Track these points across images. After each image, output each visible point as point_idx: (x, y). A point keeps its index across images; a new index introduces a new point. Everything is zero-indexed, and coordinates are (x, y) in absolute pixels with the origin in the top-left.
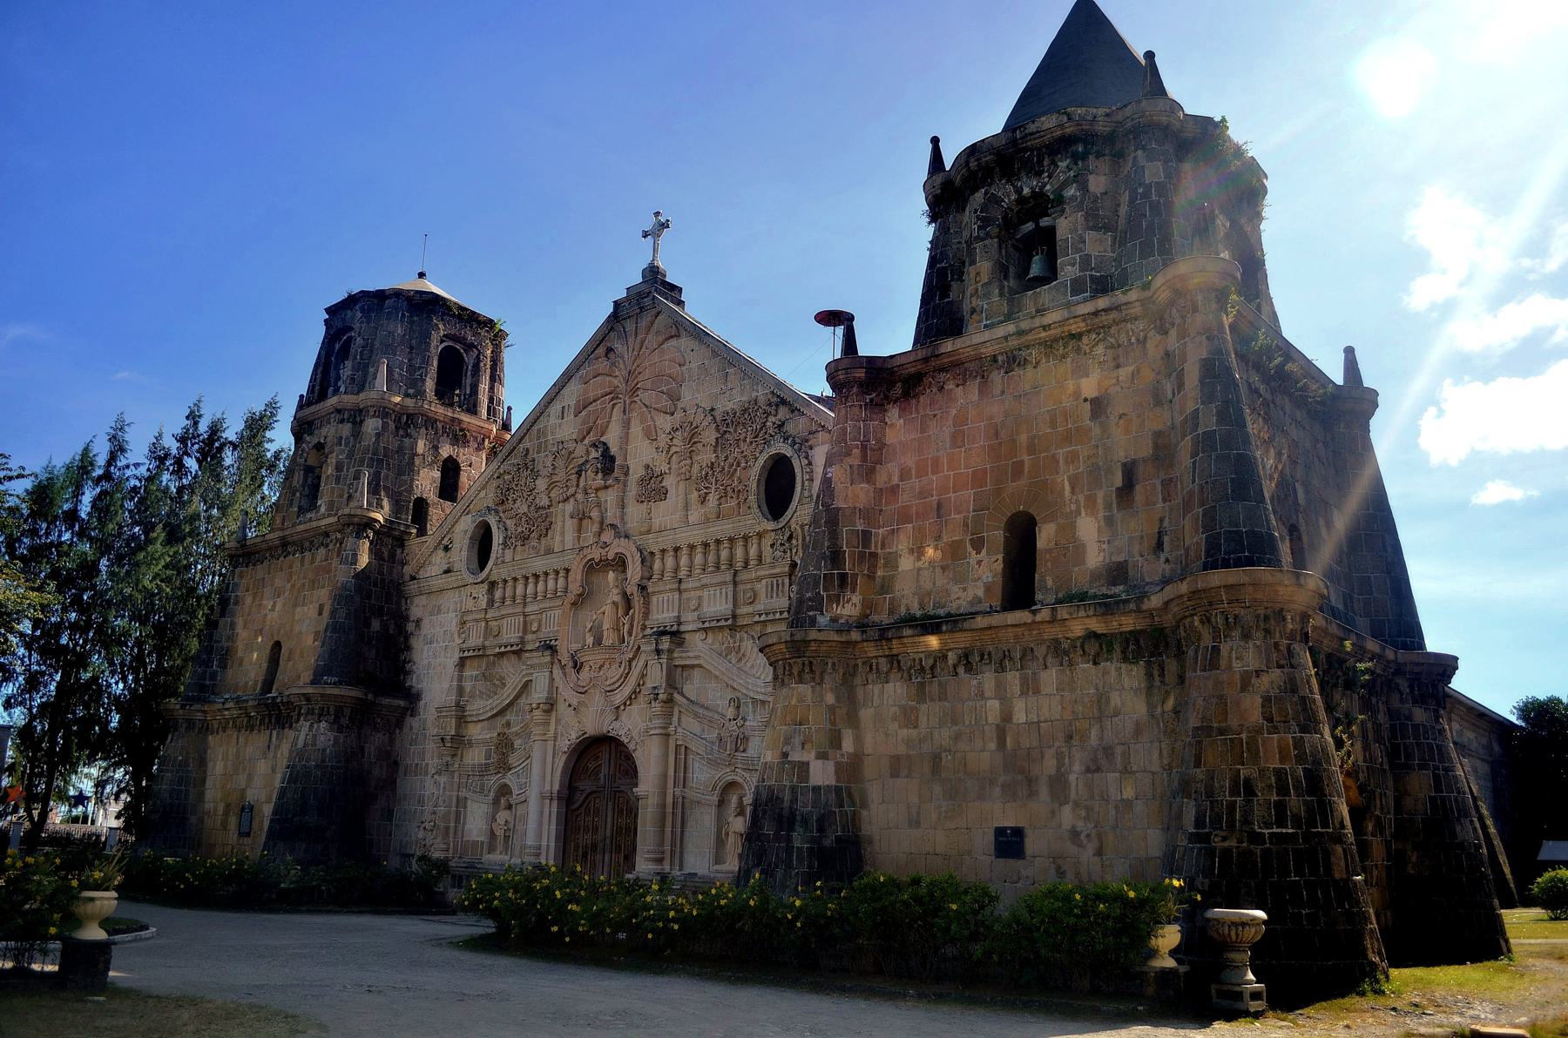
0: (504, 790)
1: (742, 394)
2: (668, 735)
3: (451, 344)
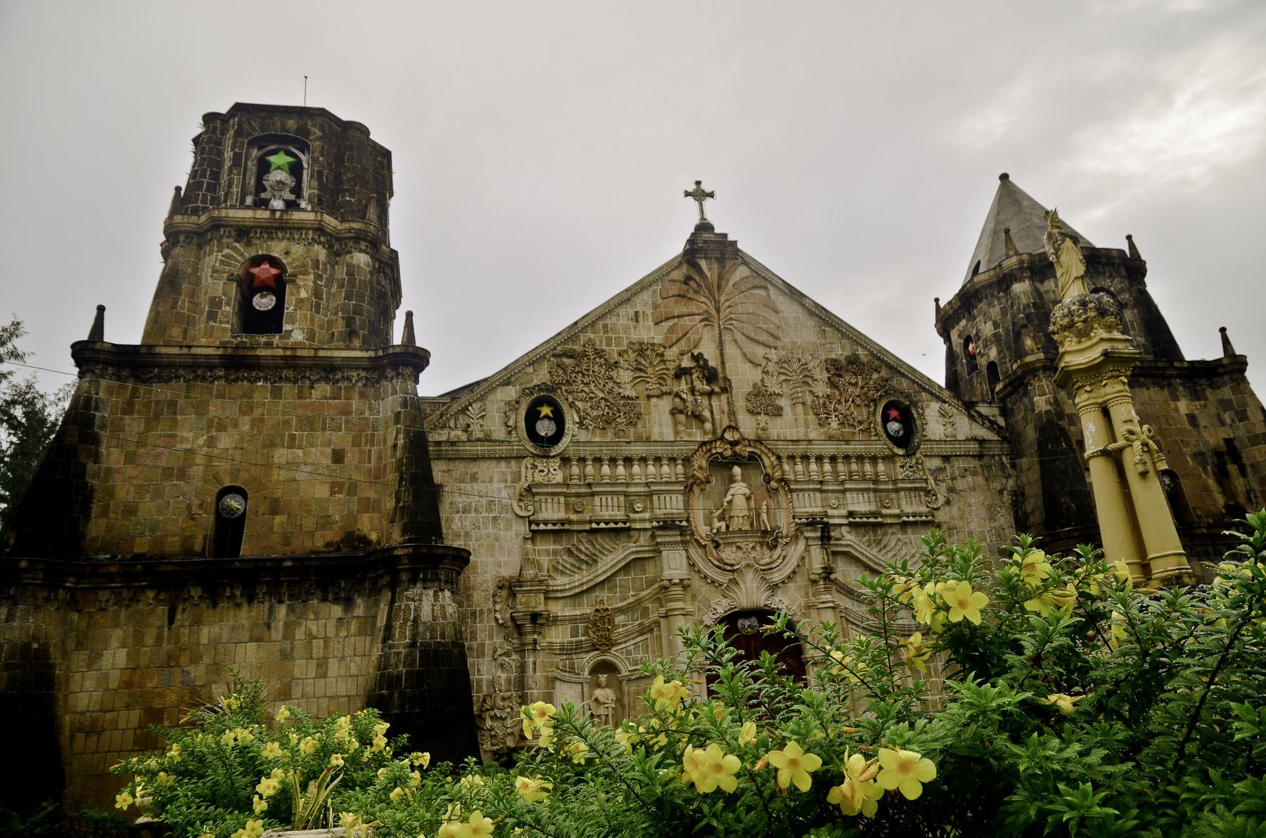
1: (843, 348)
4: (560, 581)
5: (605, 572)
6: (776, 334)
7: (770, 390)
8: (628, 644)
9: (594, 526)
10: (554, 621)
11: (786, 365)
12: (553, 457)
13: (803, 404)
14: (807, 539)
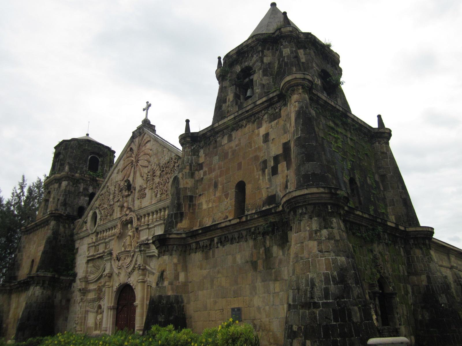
0: (100, 307)
2: (144, 282)
3: (94, 155)
10: (90, 291)
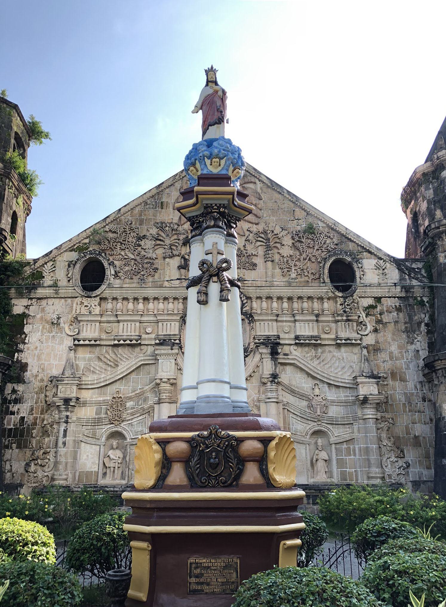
4: (89, 378)
5: (122, 373)
6: (258, 215)
7: (249, 252)
8: (133, 421)
9: (116, 342)
10: (85, 404)
11: (263, 236)
12: (94, 297)
13: (272, 261)
14: (261, 354)
